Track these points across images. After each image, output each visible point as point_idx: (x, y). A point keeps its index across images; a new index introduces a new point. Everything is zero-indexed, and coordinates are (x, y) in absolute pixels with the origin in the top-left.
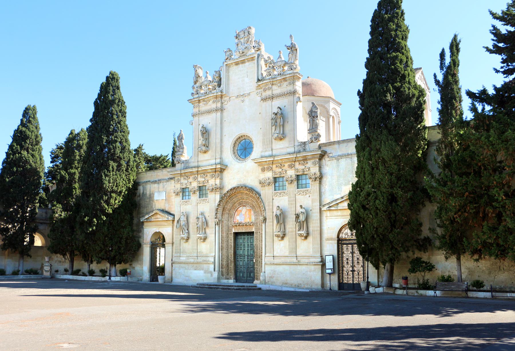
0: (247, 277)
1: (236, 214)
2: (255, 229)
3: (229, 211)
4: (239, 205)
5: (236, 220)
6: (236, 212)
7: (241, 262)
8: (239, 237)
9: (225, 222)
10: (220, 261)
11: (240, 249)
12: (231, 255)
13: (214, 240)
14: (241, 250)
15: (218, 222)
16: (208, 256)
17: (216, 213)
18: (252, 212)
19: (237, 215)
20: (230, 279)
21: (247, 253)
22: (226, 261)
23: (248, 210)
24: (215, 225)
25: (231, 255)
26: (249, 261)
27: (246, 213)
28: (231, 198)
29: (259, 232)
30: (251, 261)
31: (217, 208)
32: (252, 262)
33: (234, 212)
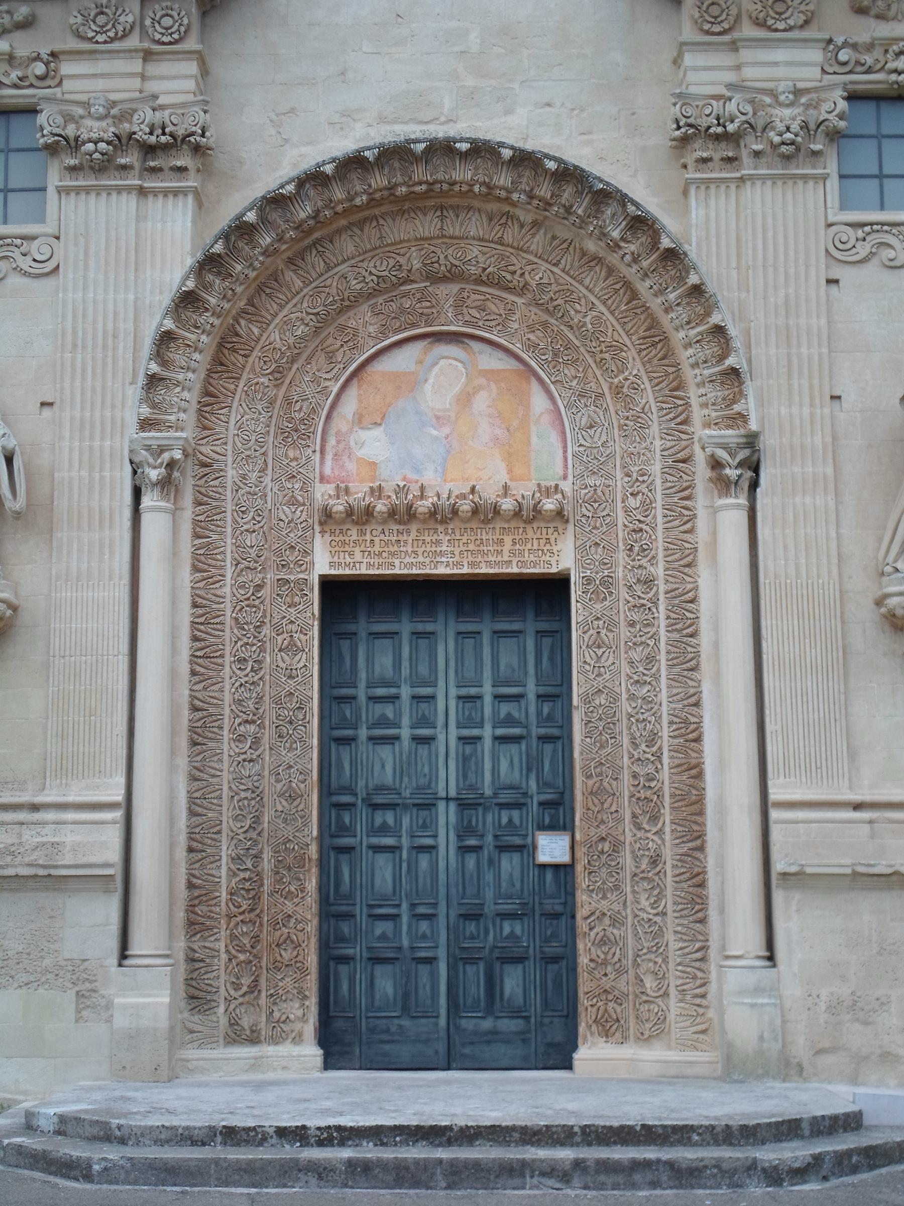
0: (454, 1007)
1: (349, 406)
2: (580, 549)
3: (278, 375)
4: (384, 332)
5: (351, 466)
6: (353, 392)
7: (382, 859)
8: (363, 626)
9: (231, 474)
10: (181, 853)
11: (374, 740)
12: (291, 796)
13: (125, 647)
14: (385, 752)
15: (171, 465)
16: (35, 808)
17: (153, 381)
18: (539, 402)
19: (359, 420)
20: (275, 1040)
21: (464, 773)
22: (234, 859)
23: (488, 374)
24: (137, 493)
25: (291, 796)
26: (476, 849)
27: (465, 399)
28: (312, 258)
29: (649, 582)
30: (503, 848)
31: (169, 324)
32: (509, 864)
33: (335, 389)
